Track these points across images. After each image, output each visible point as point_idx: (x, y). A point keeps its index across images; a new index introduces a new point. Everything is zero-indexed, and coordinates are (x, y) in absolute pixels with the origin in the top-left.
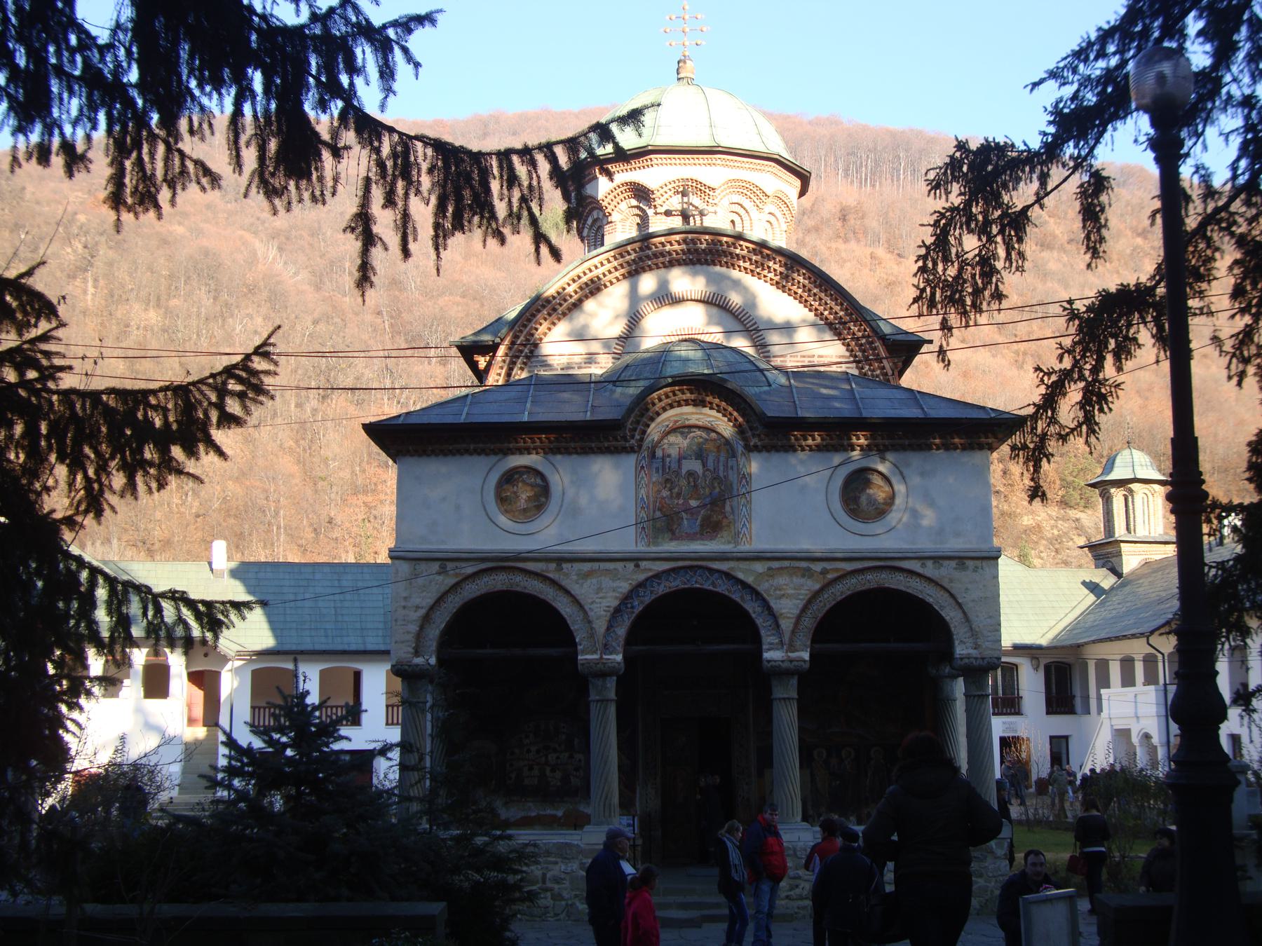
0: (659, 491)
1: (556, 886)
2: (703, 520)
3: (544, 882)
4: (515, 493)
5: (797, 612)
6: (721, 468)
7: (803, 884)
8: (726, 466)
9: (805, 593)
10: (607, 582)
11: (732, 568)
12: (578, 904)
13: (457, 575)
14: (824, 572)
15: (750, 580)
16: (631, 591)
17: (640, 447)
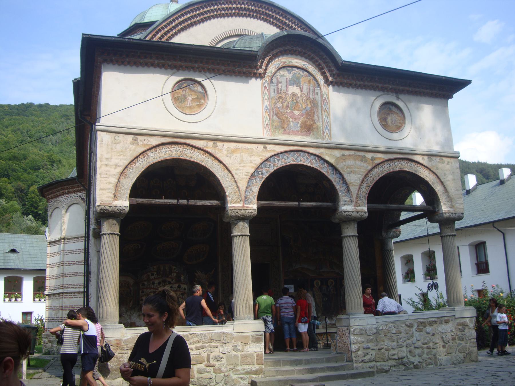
0: (275, 104)
1: (217, 363)
2: (302, 123)
3: (208, 361)
4: (184, 95)
6: (311, 93)
7: (371, 352)
9: (363, 172)
10: (246, 156)
12: (232, 375)
13: (145, 145)
14: (373, 159)
15: (332, 161)
16: (261, 164)
17: (265, 73)
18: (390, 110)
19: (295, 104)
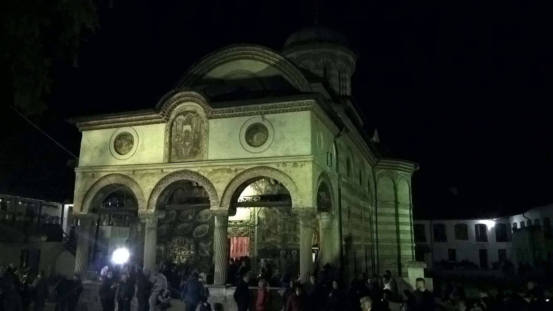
2: (191, 150)
5: (224, 188)
8: (200, 127)
9: (227, 181)
11: (199, 170)
14: (236, 170)
15: (206, 175)
16: (160, 182)
18: (257, 129)
19: (186, 139)
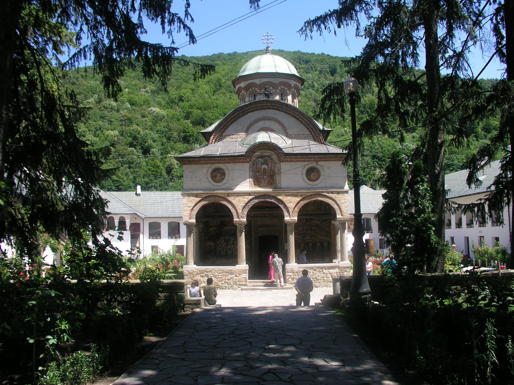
8: (274, 168)
18: (313, 170)
